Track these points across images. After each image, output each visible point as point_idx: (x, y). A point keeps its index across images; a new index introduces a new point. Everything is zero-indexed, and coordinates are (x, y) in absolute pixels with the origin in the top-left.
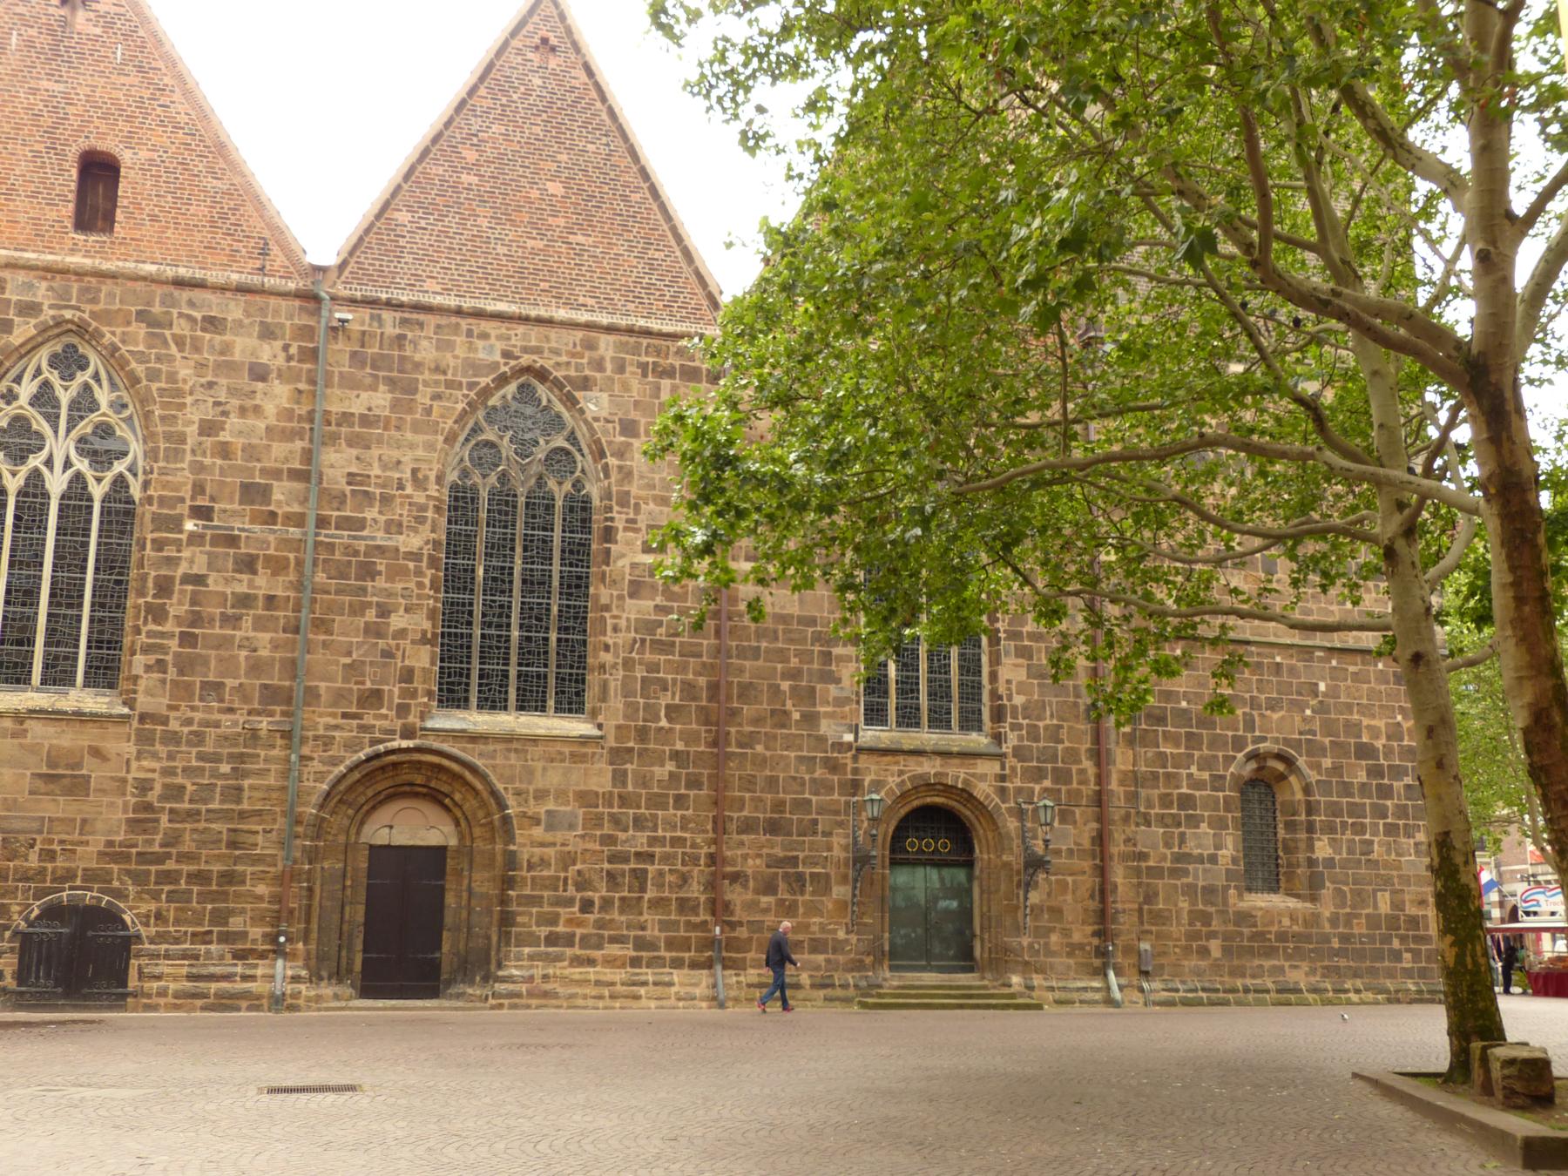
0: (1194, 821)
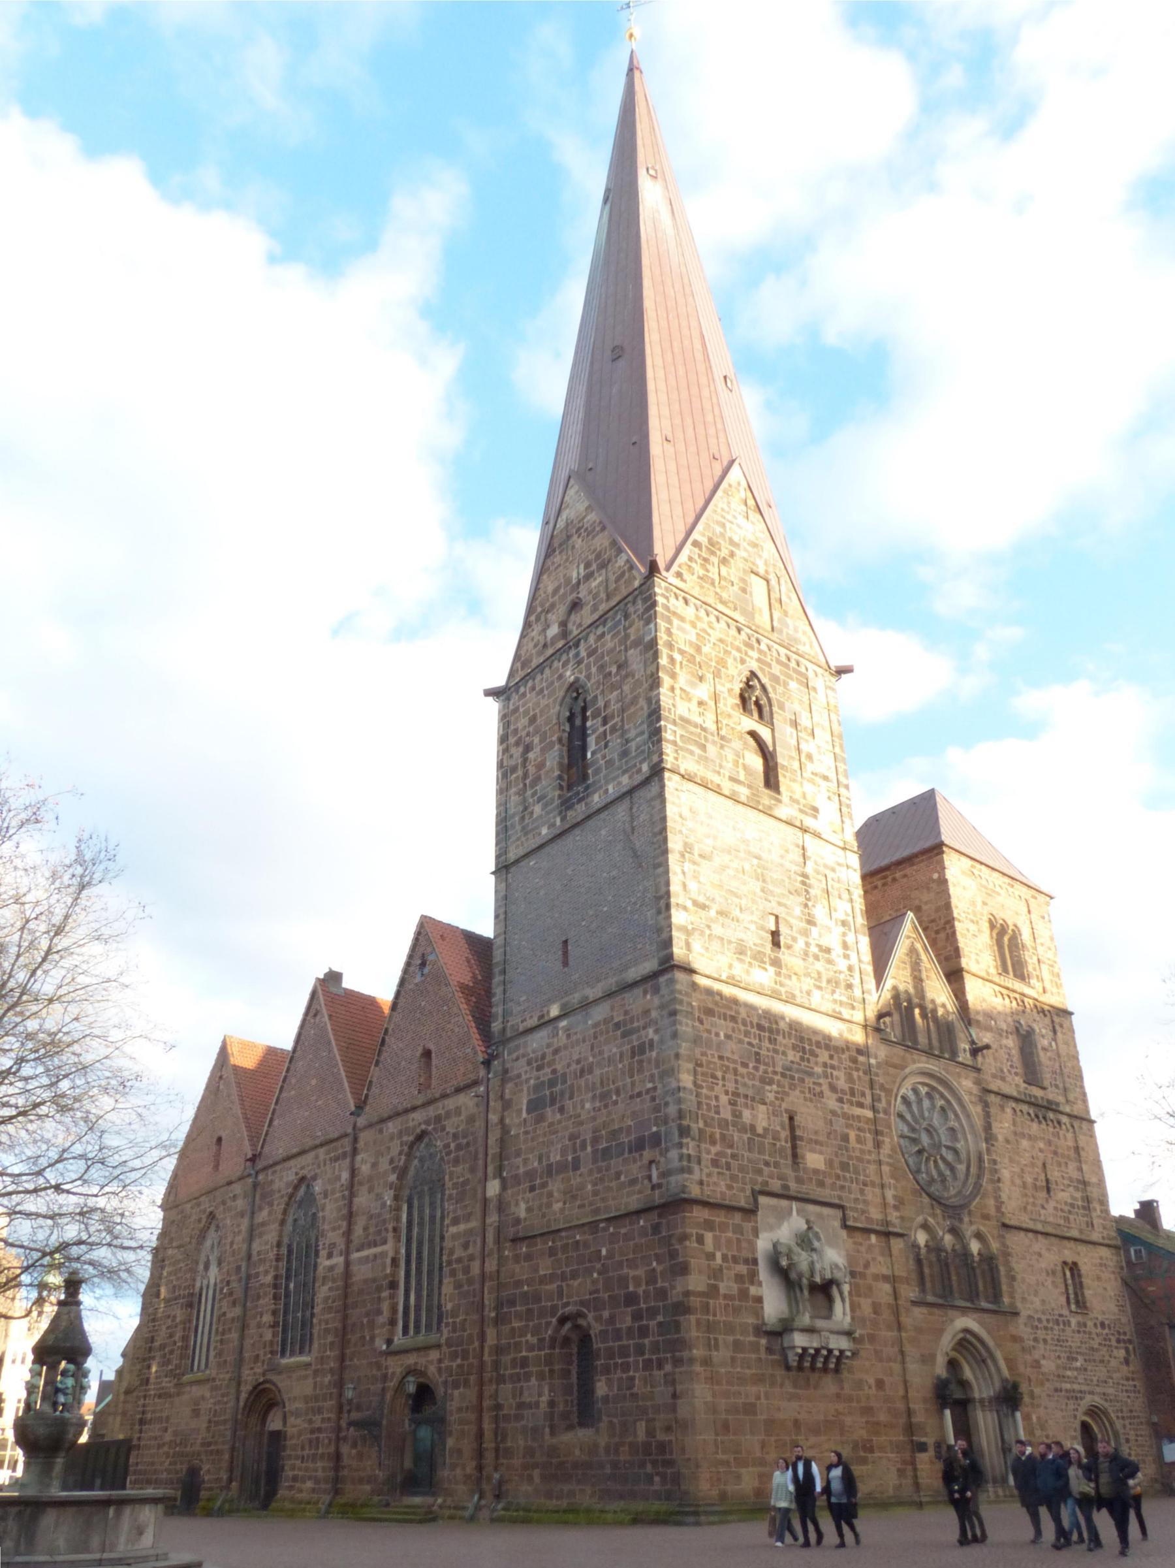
0: (528, 1376)
